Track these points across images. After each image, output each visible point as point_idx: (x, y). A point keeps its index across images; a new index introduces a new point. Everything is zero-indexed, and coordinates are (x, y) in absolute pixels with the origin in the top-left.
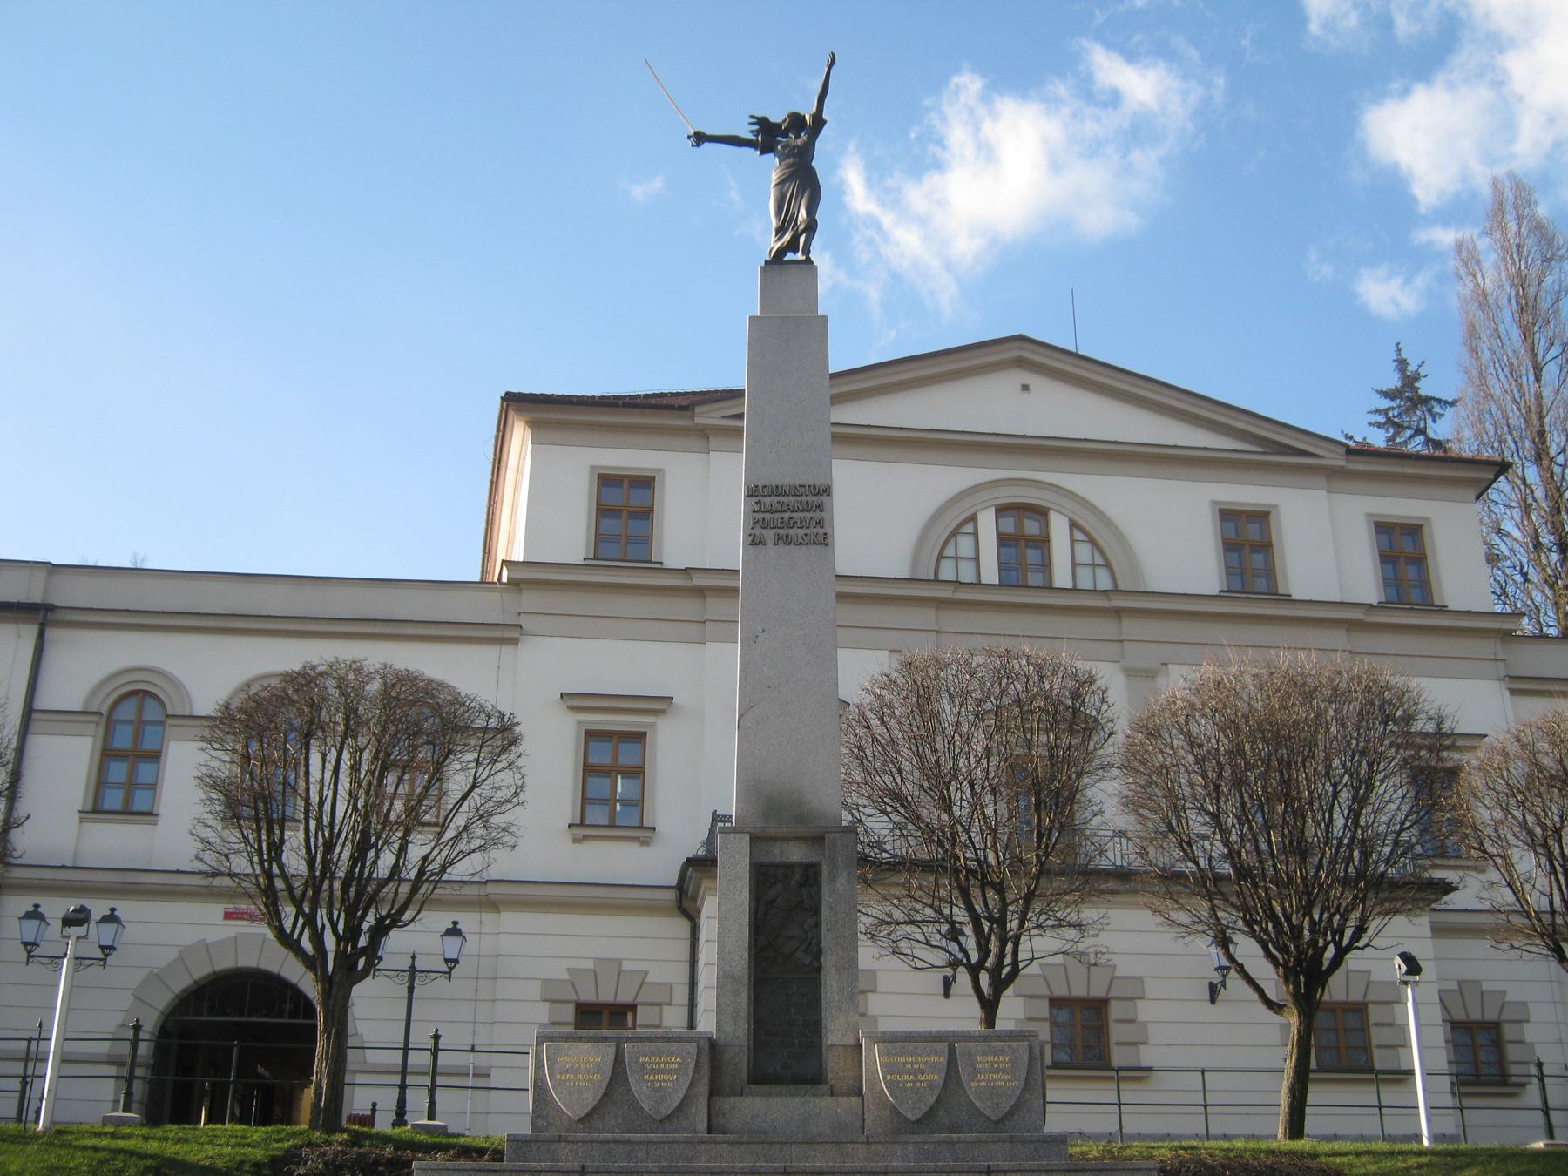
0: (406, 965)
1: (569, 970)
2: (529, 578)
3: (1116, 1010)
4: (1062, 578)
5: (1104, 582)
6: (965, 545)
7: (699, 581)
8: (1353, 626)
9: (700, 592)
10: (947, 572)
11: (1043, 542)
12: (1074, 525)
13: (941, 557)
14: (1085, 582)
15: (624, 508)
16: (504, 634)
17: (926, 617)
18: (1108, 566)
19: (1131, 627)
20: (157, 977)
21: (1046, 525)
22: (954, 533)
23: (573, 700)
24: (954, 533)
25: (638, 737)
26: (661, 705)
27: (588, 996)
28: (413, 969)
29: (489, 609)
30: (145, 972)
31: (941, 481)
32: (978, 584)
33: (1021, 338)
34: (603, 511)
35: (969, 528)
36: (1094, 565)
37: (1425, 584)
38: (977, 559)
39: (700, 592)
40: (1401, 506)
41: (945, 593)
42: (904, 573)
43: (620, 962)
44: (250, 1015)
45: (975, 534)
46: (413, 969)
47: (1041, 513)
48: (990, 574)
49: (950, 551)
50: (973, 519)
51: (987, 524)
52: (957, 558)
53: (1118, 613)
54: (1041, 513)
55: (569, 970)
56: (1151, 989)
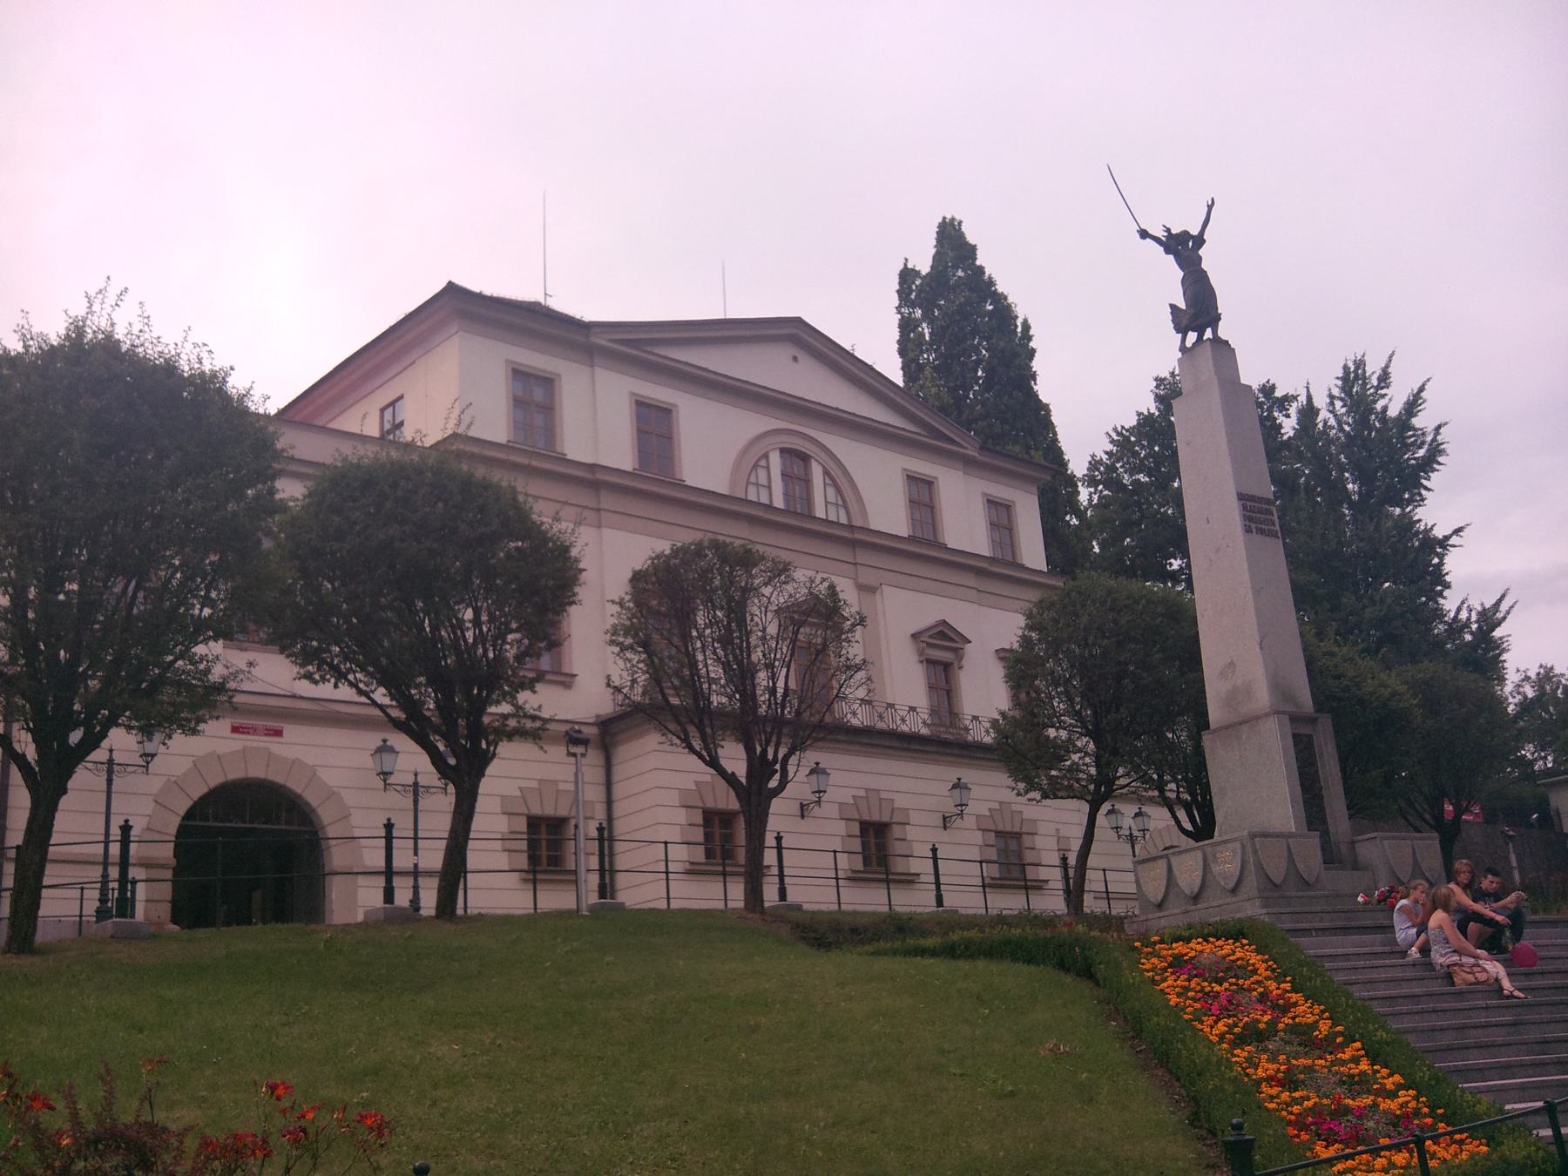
0: (411, 780)
1: (521, 789)
3: (896, 831)
4: (820, 512)
5: (844, 520)
6: (762, 474)
7: (600, 476)
8: (980, 572)
10: (752, 497)
11: (807, 482)
12: (826, 473)
14: (832, 517)
18: (845, 506)
19: (863, 557)
20: (177, 784)
21: (807, 468)
22: (756, 466)
27: (536, 810)
28: (416, 784)
30: (164, 779)
31: (753, 423)
33: (798, 321)
35: (763, 463)
36: (836, 504)
38: (769, 487)
42: (725, 491)
43: (555, 782)
44: (251, 822)
45: (768, 468)
46: (416, 784)
47: (805, 458)
48: (779, 502)
49: (753, 479)
50: (766, 456)
51: (775, 460)
52: (757, 485)
53: (853, 544)
54: (805, 458)
55: (521, 789)
56: (914, 817)
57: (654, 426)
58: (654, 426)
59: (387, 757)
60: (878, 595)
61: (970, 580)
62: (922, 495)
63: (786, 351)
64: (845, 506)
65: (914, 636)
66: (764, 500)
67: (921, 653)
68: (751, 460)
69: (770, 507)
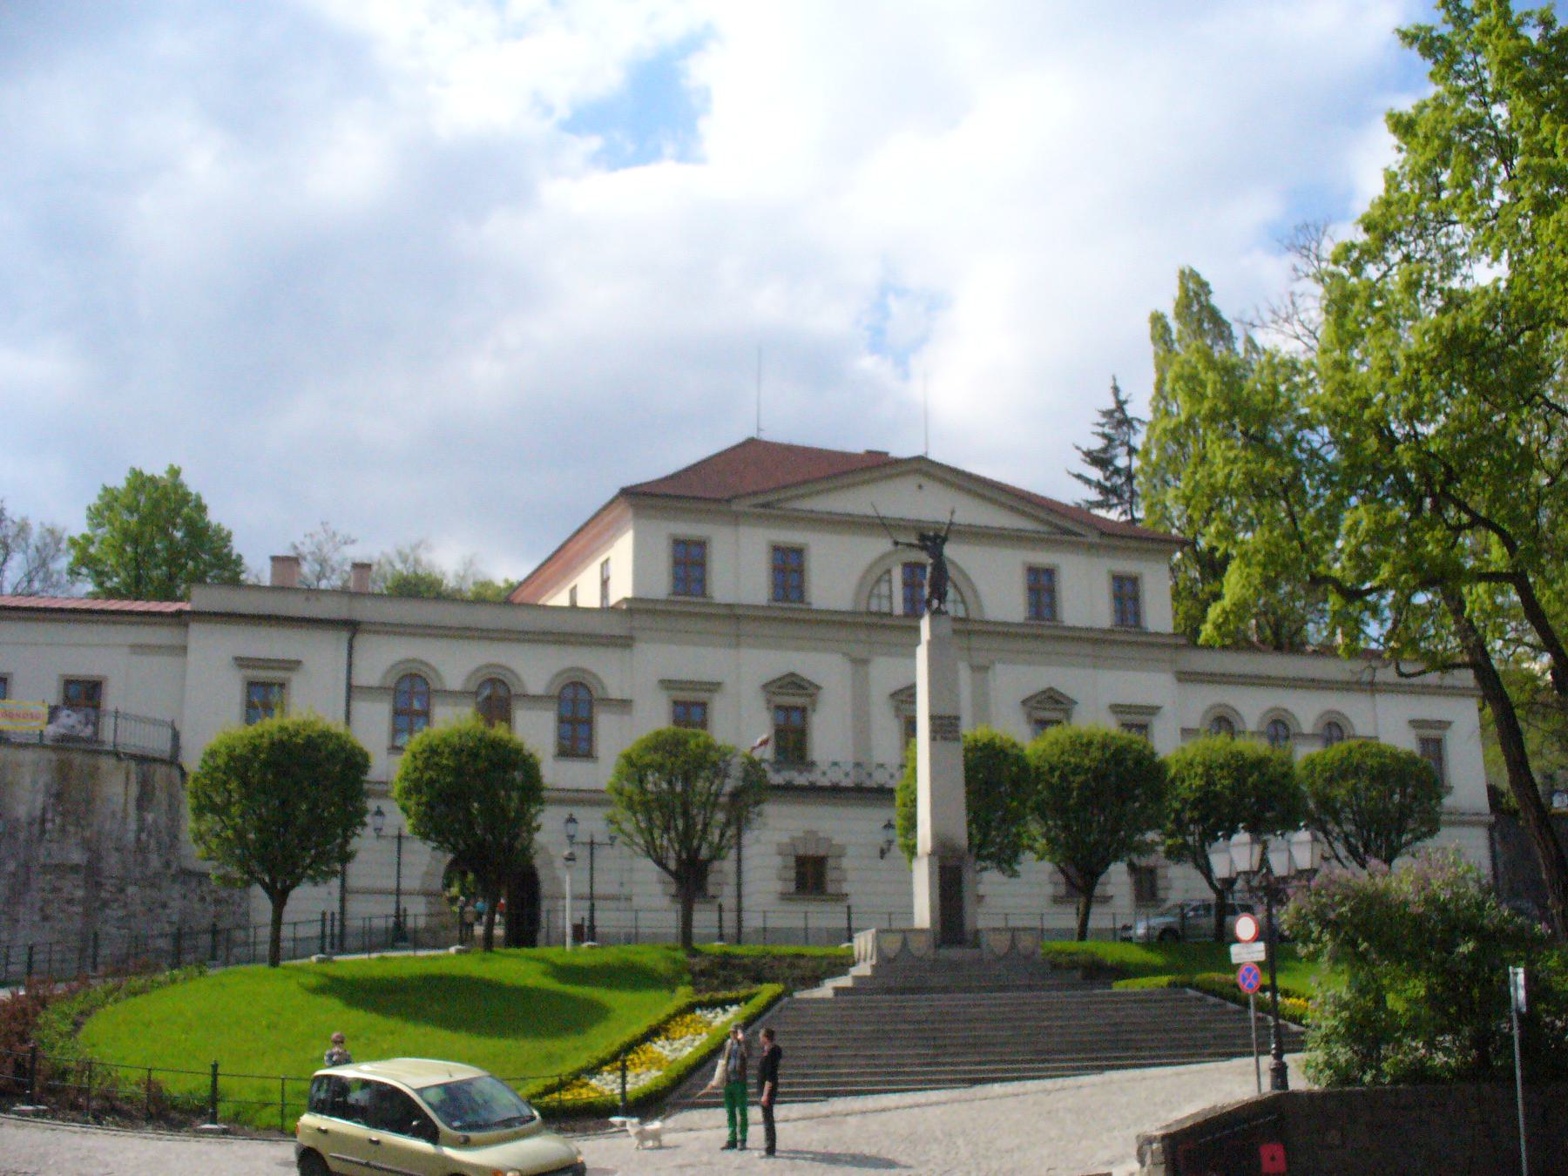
2: (635, 608)
6: (884, 588)
8: (1095, 642)
9: (738, 618)
10: (874, 607)
13: (870, 597)
15: (689, 563)
16: (624, 642)
17: (863, 635)
18: (963, 602)
19: (975, 642)
22: (878, 581)
23: (668, 684)
24: (878, 581)
25: (703, 706)
26: (714, 687)
29: (617, 628)
32: (890, 614)
34: (677, 563)
37: (1137, 614)
38: (890, 597)
39: (738, 618)
40: (1126, 566)
41: (875, 620)
45: (890, 581)
50: (889, 572)
51: (897, 575)
52: (879, 596)
57: (788, 568)
58: (788, 568)
59: (571, 826)
60: (990, 673)
61: (1087, 649)
62: (1042, 585)
63: (911, 482)
64: (963, 602)
65: (1024, 702)
66: (885, 609)
67: (1029, 715)
68: (876, 576)
69: (890, 614)
